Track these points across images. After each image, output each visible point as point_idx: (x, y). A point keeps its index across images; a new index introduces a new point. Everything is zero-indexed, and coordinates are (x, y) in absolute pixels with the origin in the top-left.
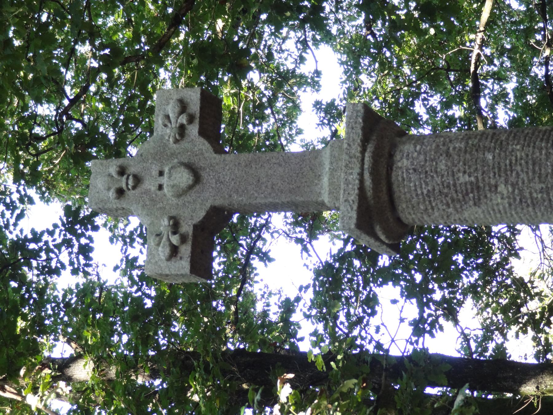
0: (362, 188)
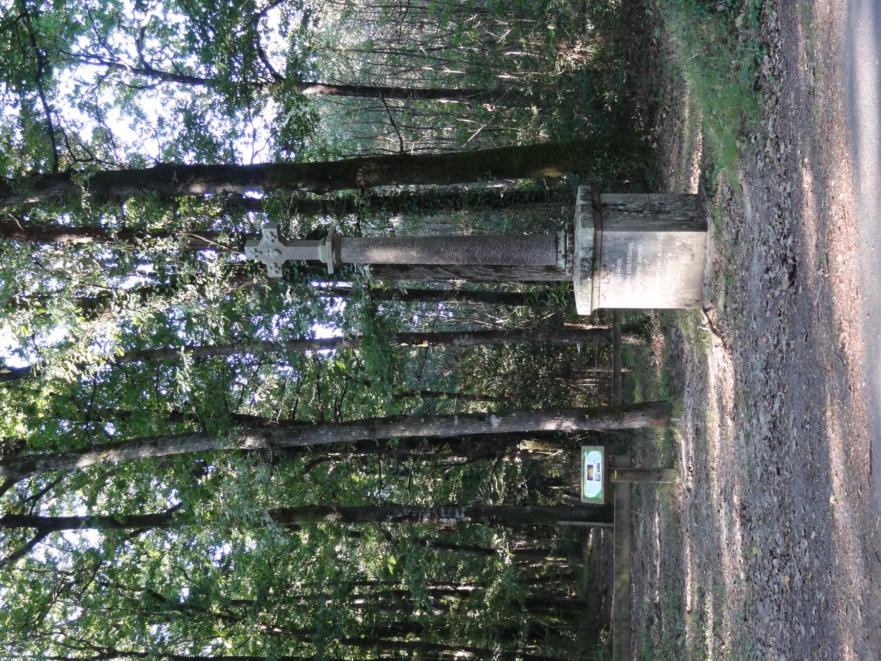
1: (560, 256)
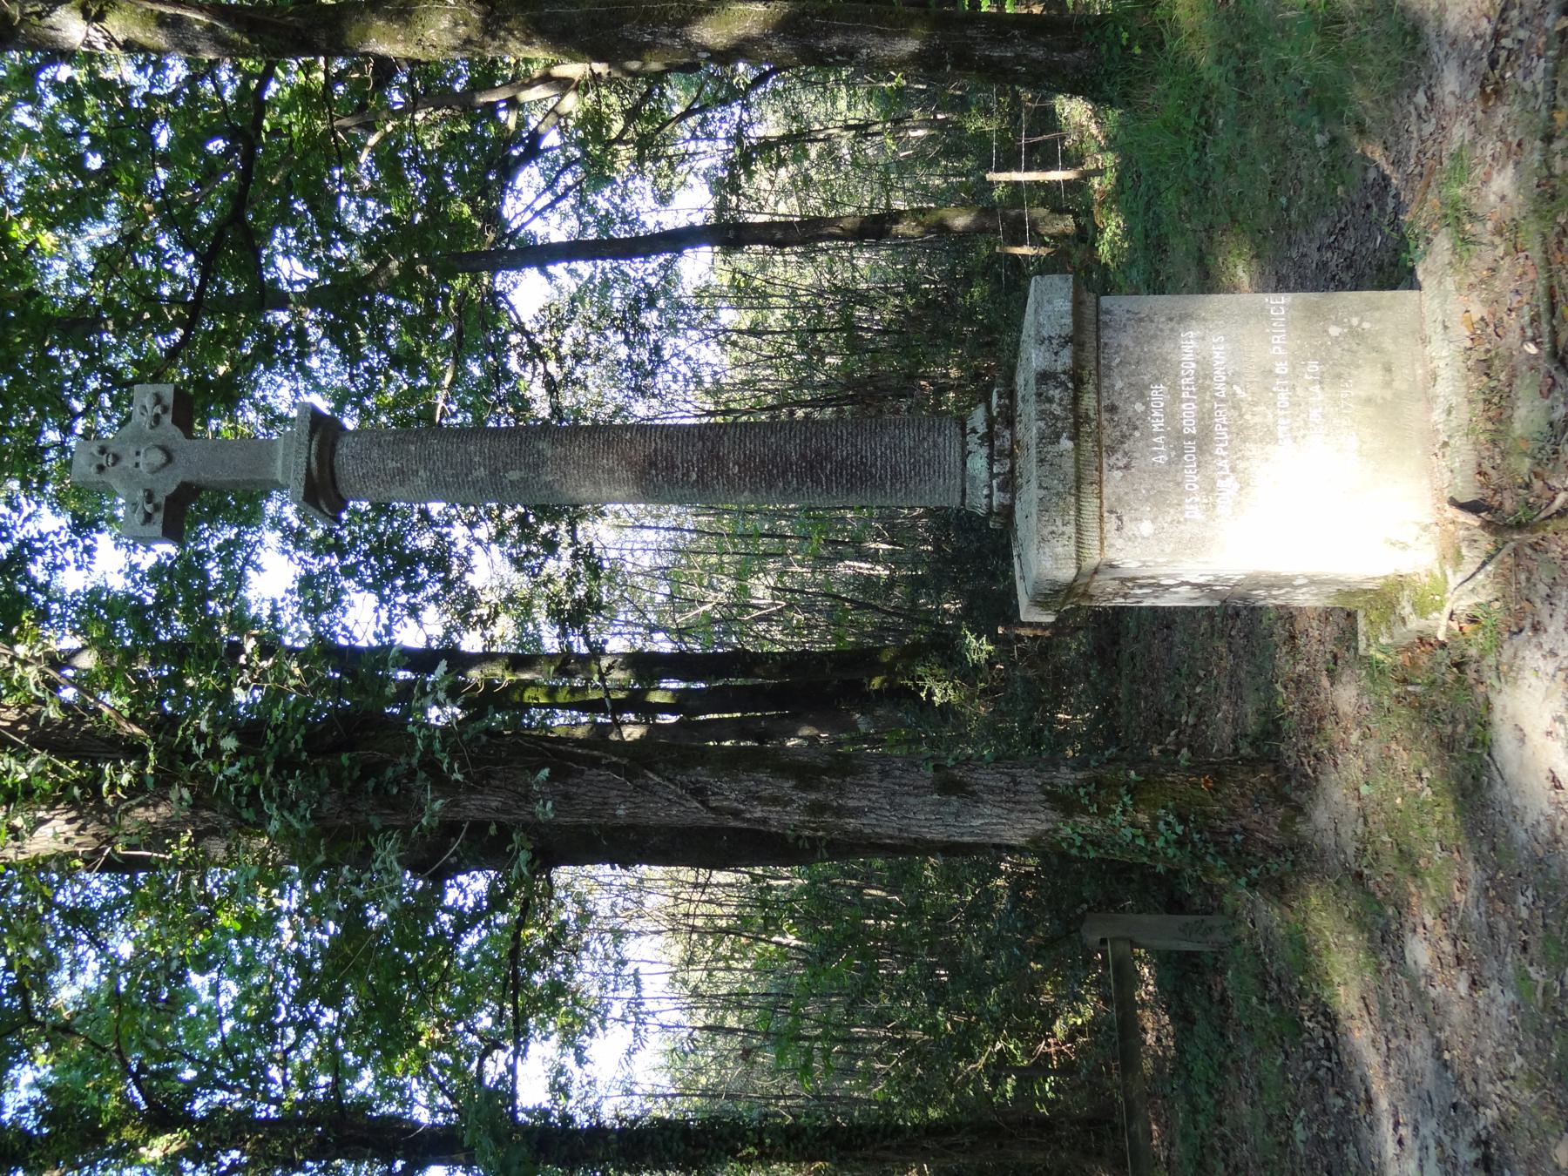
0: (309, 469)
1: (973, 440)
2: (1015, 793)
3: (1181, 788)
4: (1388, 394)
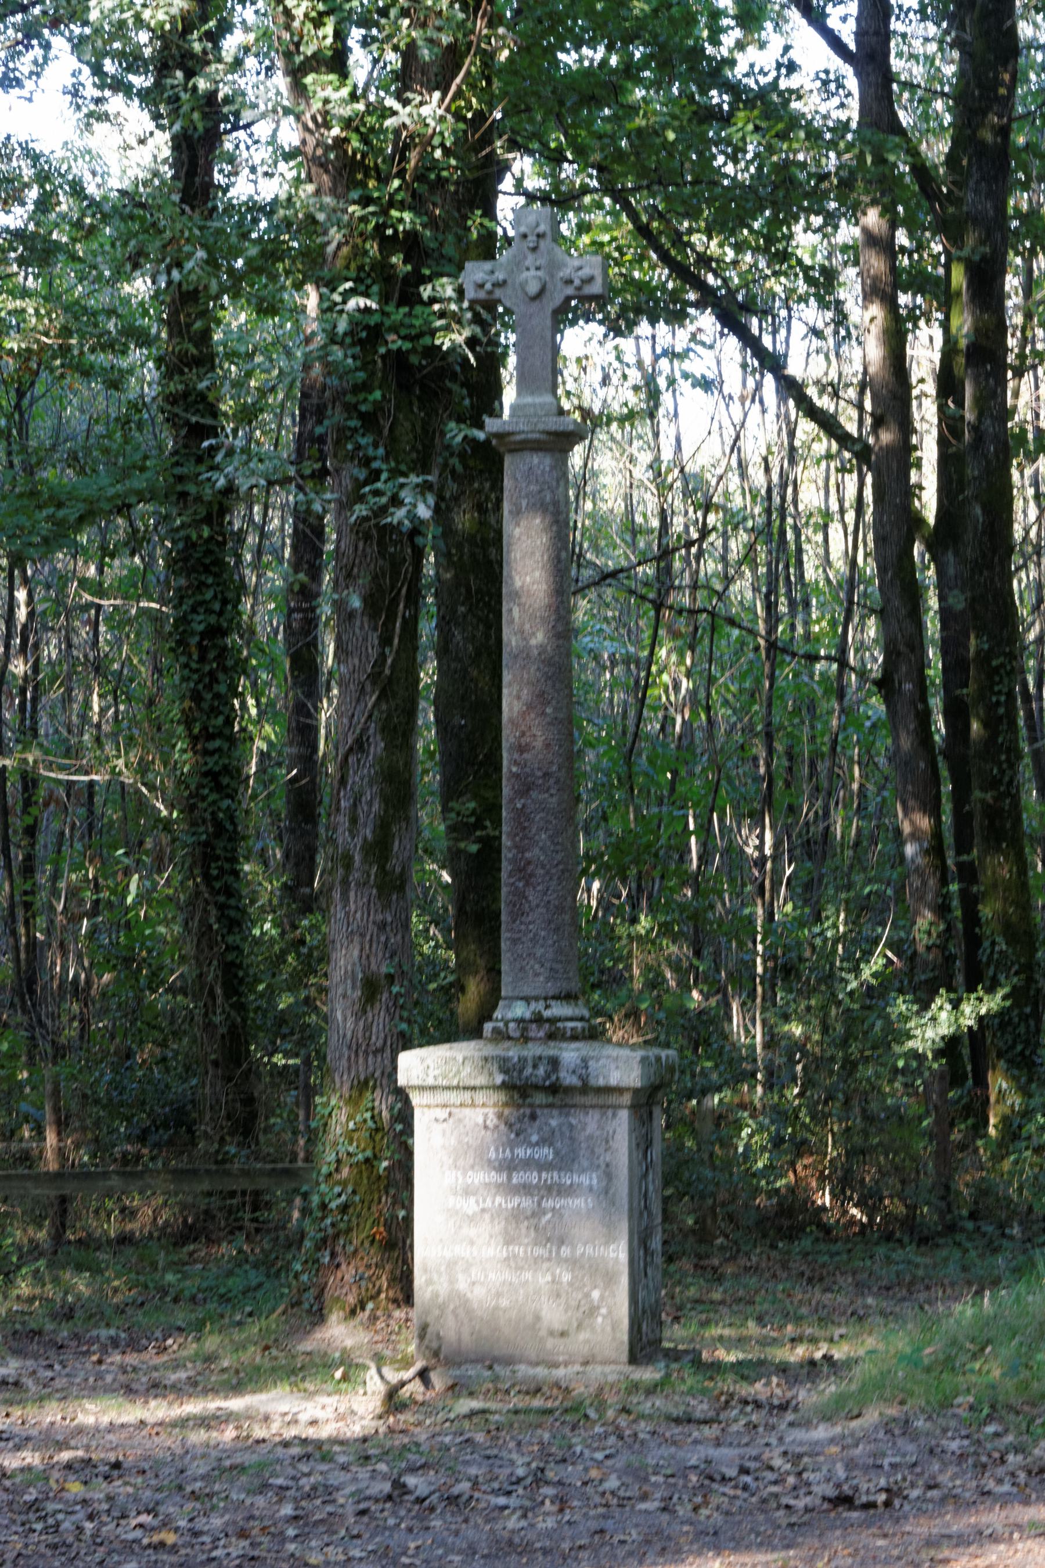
1: (540, 1006)
2: (366, 1053)
3: (374, 1209)
4: (543, 1333)
